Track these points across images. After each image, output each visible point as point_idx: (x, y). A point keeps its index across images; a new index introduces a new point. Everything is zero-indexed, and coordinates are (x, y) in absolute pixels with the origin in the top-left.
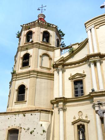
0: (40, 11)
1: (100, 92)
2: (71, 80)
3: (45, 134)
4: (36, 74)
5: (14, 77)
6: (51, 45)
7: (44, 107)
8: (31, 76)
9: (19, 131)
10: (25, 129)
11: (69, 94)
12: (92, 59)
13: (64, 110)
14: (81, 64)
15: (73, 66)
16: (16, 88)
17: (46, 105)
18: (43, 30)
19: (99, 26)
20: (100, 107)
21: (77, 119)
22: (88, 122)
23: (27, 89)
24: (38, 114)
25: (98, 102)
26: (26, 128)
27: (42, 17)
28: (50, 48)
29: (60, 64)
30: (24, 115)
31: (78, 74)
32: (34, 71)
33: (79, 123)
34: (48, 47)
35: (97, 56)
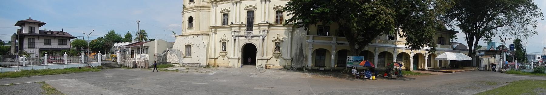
1: (236, 25)
3: (206, 47)
4: (199, 8)
7: (205, 31)
8: (196, 10)
11: (219, 23)
17: (206, 30)
23: (194, 19)
24: (201, 36)
26: (195, 44)
32: (198, 7)
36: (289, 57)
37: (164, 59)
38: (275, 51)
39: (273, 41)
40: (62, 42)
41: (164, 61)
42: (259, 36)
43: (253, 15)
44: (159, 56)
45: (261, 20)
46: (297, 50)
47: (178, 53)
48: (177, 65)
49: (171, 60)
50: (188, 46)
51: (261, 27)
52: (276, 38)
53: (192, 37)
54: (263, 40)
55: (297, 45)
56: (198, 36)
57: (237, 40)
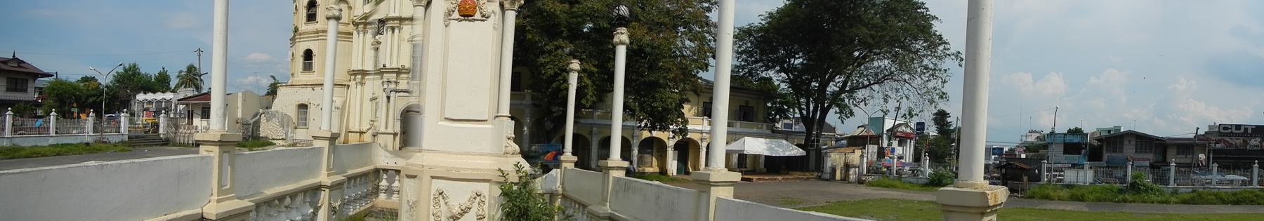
9: (309, 107)
13: (362, 84)
16: (301, 53)
37: (254, 130)
40: (16, 86)
41: (255, 135)
44: (245, 124)
48: (282, 143)
49: (269, 132)
50: (303, 107)
53: (309, 89)
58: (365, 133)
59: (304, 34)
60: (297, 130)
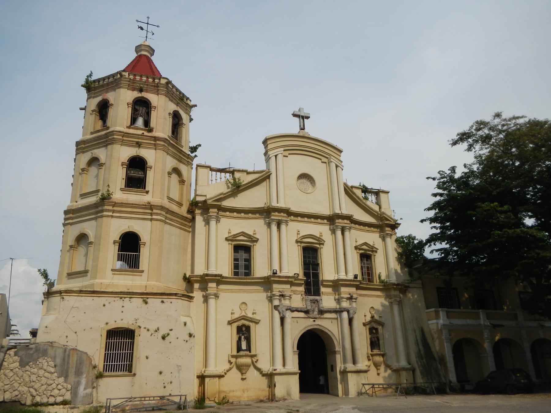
0: (144, 32)
2: (230, 242)
4: (164, 213)
5: (106, 207)
6: (182, 146)
10: (148, 330)
12: (275, 216)
14: (250, 215)
15: (235, 214)
16: (116, 236)
18: (172, 107)
19: (289, 154)
20: (280, 300)
21: (236, 316)
22: (257, 322)
23: (144, 244)
25: (280, 292)
26: (153, 328)
27: (149, 56)
28: (184, 155)
29: (214, 206)
30: (144, 301)
31: (243, 234)
33: (240, 323)
34: (180, 153)
35: (284, 213)
36: (403, 363)
38: (372, 351)
39: (364, 325)
42: (338, 312)
43: (316, 257)
45: (337, 271)
46: (418, 344)
47: (66, 359)
51: (343, 289)
52: (368, 318)
53: (138, 301)
54: (351, 320)
55: (415, 333)
56: (164, 300)
57: (288, 321)
58: (223, 376)
59: (122, 205)
60: (103, 382)
